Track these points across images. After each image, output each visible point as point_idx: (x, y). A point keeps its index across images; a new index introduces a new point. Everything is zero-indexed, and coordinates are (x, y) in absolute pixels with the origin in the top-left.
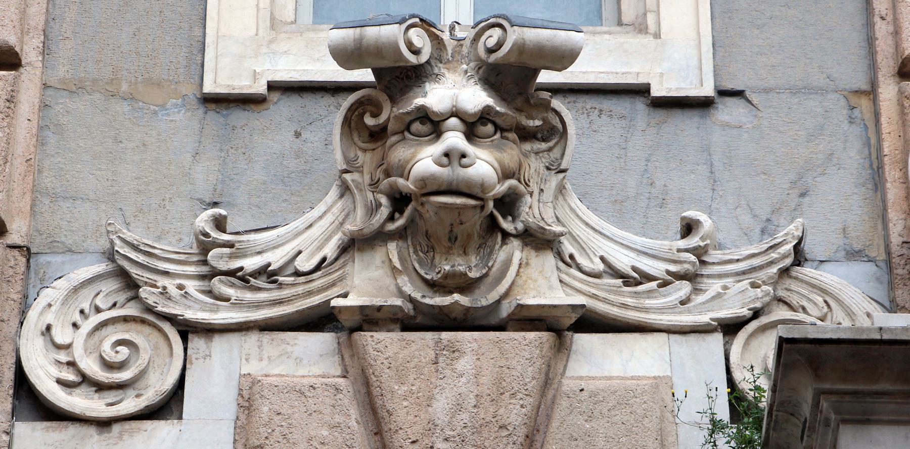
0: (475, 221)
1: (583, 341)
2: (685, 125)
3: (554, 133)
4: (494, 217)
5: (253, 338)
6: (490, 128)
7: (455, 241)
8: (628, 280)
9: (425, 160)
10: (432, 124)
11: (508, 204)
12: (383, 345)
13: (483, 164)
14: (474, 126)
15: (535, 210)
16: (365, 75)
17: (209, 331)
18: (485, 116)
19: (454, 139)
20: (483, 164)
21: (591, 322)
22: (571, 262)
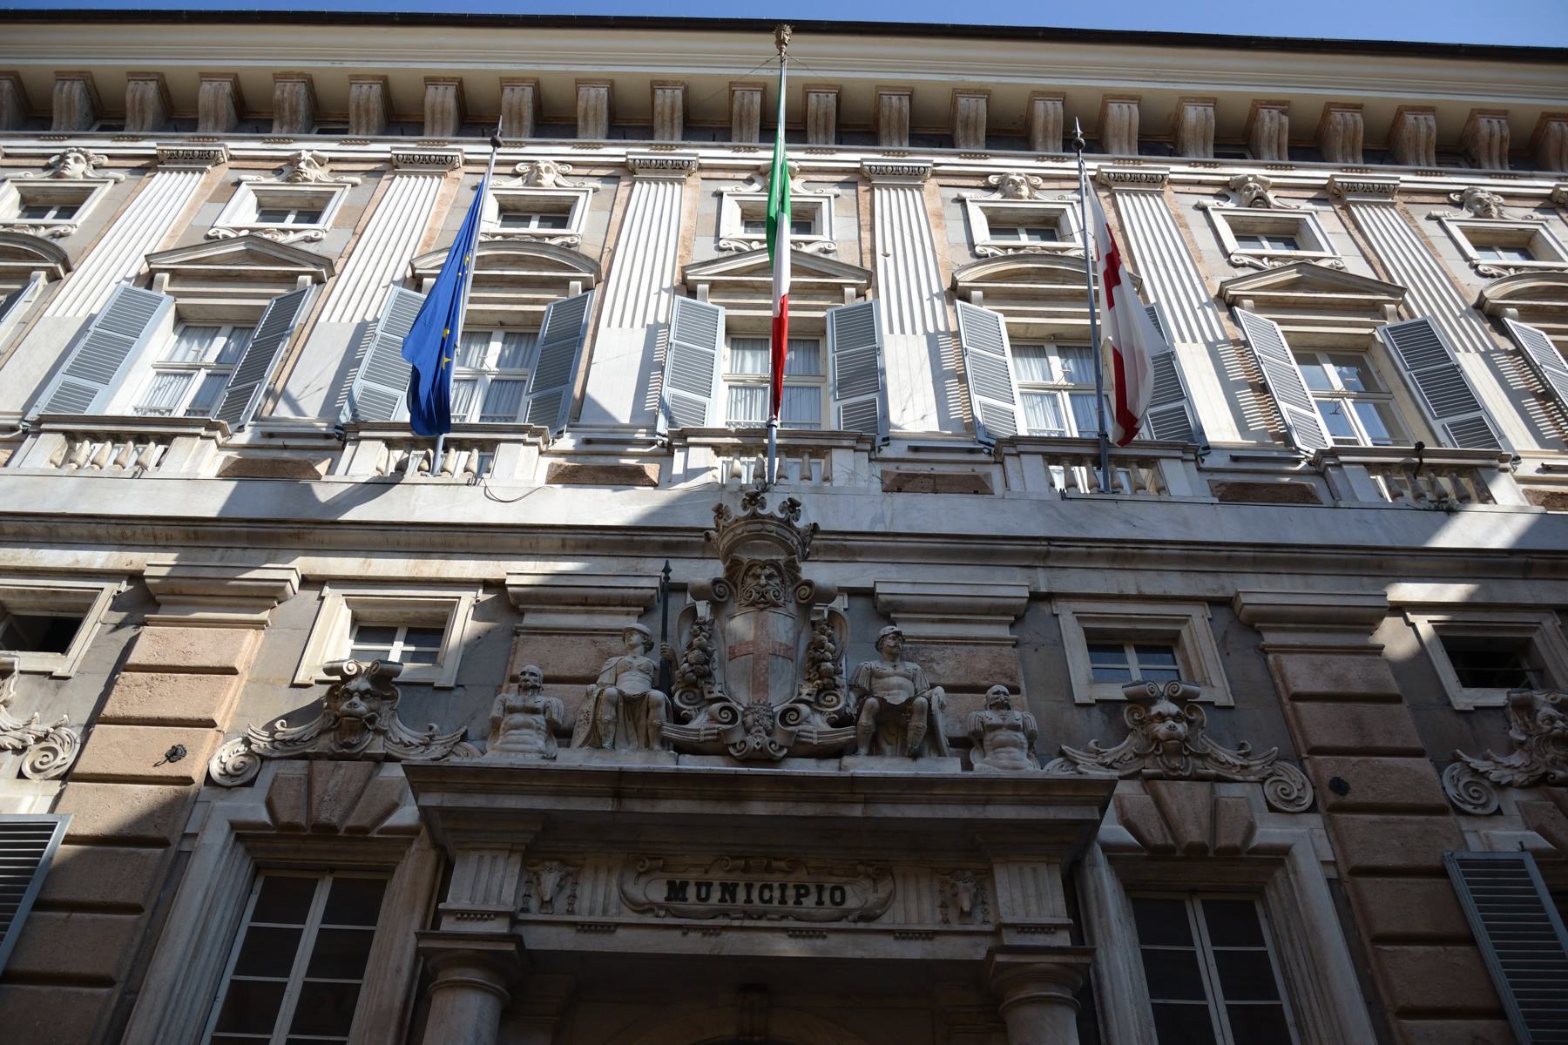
1: (388, 765)
2: (444, 695)
3: (394, 698)
4: (365, 724)
5: (283, 762)
7: (353, 732)
9: (344, 707)
11: (372, 720)
12: (320, 765)
13: (362, 707)
14: (363, 695)
15: (382, 723)
16: (338, 678)
17: (270, 759)
18: (367, 691)
19: (356, 699)
20: (362, 707)
21: (389, 758)
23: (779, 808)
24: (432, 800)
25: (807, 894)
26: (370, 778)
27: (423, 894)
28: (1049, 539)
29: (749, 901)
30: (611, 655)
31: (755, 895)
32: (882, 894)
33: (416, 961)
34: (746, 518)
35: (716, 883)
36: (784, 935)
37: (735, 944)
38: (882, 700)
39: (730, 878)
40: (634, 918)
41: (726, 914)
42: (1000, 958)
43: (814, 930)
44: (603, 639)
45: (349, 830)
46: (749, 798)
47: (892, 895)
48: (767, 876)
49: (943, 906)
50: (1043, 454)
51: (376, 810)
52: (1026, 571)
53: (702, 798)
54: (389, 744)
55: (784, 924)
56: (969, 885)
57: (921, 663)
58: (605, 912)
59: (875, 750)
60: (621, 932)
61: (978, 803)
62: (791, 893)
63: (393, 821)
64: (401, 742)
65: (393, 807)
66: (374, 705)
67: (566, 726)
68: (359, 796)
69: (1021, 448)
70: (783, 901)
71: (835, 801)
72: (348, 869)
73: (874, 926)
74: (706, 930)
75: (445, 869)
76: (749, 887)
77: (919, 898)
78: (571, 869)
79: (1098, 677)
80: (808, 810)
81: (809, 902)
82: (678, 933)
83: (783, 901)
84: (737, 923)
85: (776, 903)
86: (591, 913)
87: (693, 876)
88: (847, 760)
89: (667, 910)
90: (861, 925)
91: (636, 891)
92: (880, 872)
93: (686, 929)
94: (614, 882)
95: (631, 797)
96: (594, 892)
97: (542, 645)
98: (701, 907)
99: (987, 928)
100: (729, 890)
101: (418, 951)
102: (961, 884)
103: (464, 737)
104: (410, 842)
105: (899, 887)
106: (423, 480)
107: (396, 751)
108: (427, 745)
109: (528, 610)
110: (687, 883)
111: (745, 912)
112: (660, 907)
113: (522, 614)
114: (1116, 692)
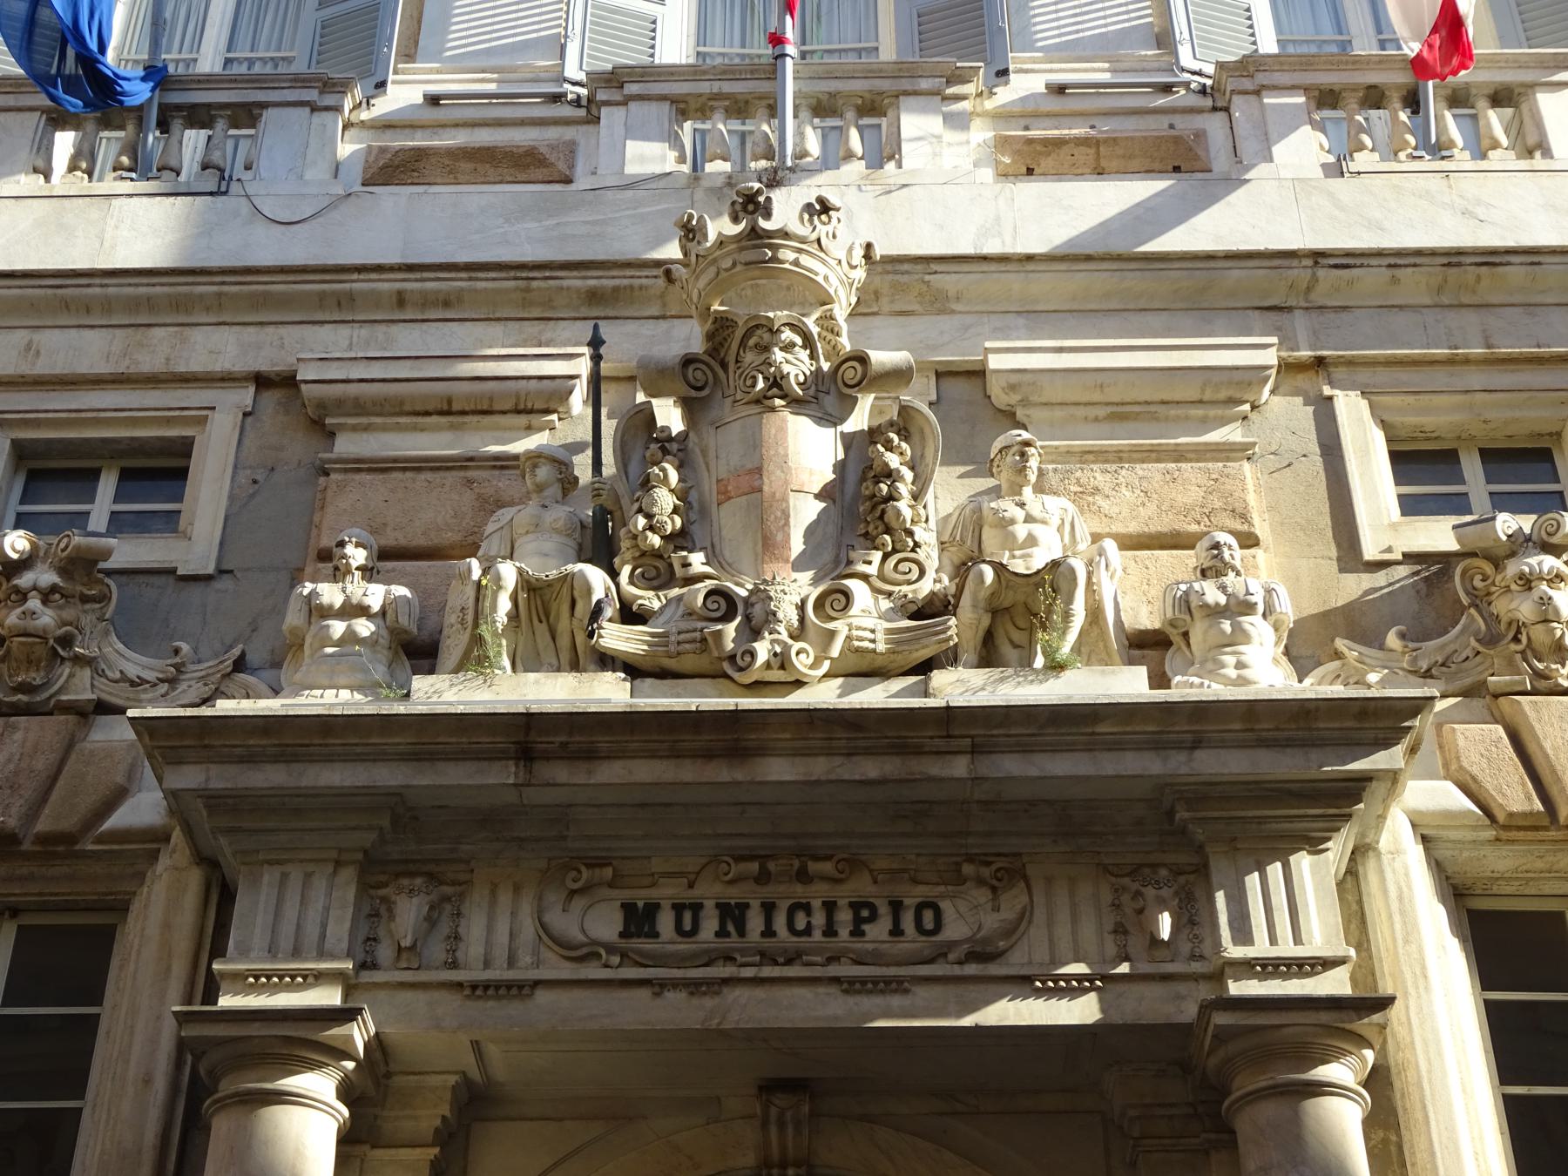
0: (41, 651)
2: (195, 592)
3: (104, 598)
6: (57, 596)
7: (31, 662)
8: (133, 684)
9: (13, 619)
10: (23, 596)
11: (66, 641)
13: (47, 618)
14: (47, 595)
18: (54, 589)
19: (34, 603)
20: (47, 618)
21: (104, 708)
22: (103, 674)
23: (819, 767)
24: (189, 777)
25: (873, 918)
26: (70, 746)
27: (183, 944)
28: (1317, 255)
29: (769, 932)
30: (500, 504)
31: (780, 923)
32: (1008, 914)
33: (178, 1064)
34: (738, 238)
35: (709, 904)
36: (834, 990)
37: (748, 1008)
38: (999, 568)
39: (734, 895)
40: (566, 971)
41: (729, 958)
42: (1221, 1019)
43: (888, 981)
44: (485, 474)
45: (43, 839)
46: (761, 751)
47: (1025, 916)
48: (799, 889)
49: (1120, 930)
50: (1306, 90)
51: (87, 801)
52: (1272, 315)
53: (676, 754)
54: (100, 682)
55: (834, 970)
56: (1166, 892)
57: (1076, 498)
58: (511, 962)
59: (988, 657)
60: (543, 997)
61: (1178, 746)
62: (844, 916)
63: (120, 819)
64: (124, 678)
65: (118, 796)
66: (69, 614)
67: (425, 635)
68: (54, 779)
69: (1261, 78)
70: (830, 931)
71: (918, 751)
72: (43, 908)
73: (994, 969)
74: (695, 987)
75: (221, 898)
76: (769, 909)
77: (1075, 920)
78: (448, 890)
79: (1410, 506)
80: (871, 769)
81: (878, 931)
82: (644, 994)
83: (830, 931)
84: (748, 972)
85: (817, 935)
86: (487, 964)
87: (668, 892)
88: (939, 678)
89: (624, 955)
90: (971, 969)
91: (566, 923)
92: (1007, 873)
93: (659, 987)
94: (526, 909)
95: (548, 757)
96: (490, 929)
97: (374, 489)
98: (684, 947)
99: (1196, 967)
100: (733, 915)
101: (182, 1045)
102: (1150, 892)
103: (240, 665)
104: (154, 856)
105: (1039, 898)
106: (126, 187)
107: (114, 696)
108: (172, 682)
109: (342, 427)
110: (657, 906)
111: (762, 954)
112: (611, 949)
113: (332, 435)
114: (1438, 535)
